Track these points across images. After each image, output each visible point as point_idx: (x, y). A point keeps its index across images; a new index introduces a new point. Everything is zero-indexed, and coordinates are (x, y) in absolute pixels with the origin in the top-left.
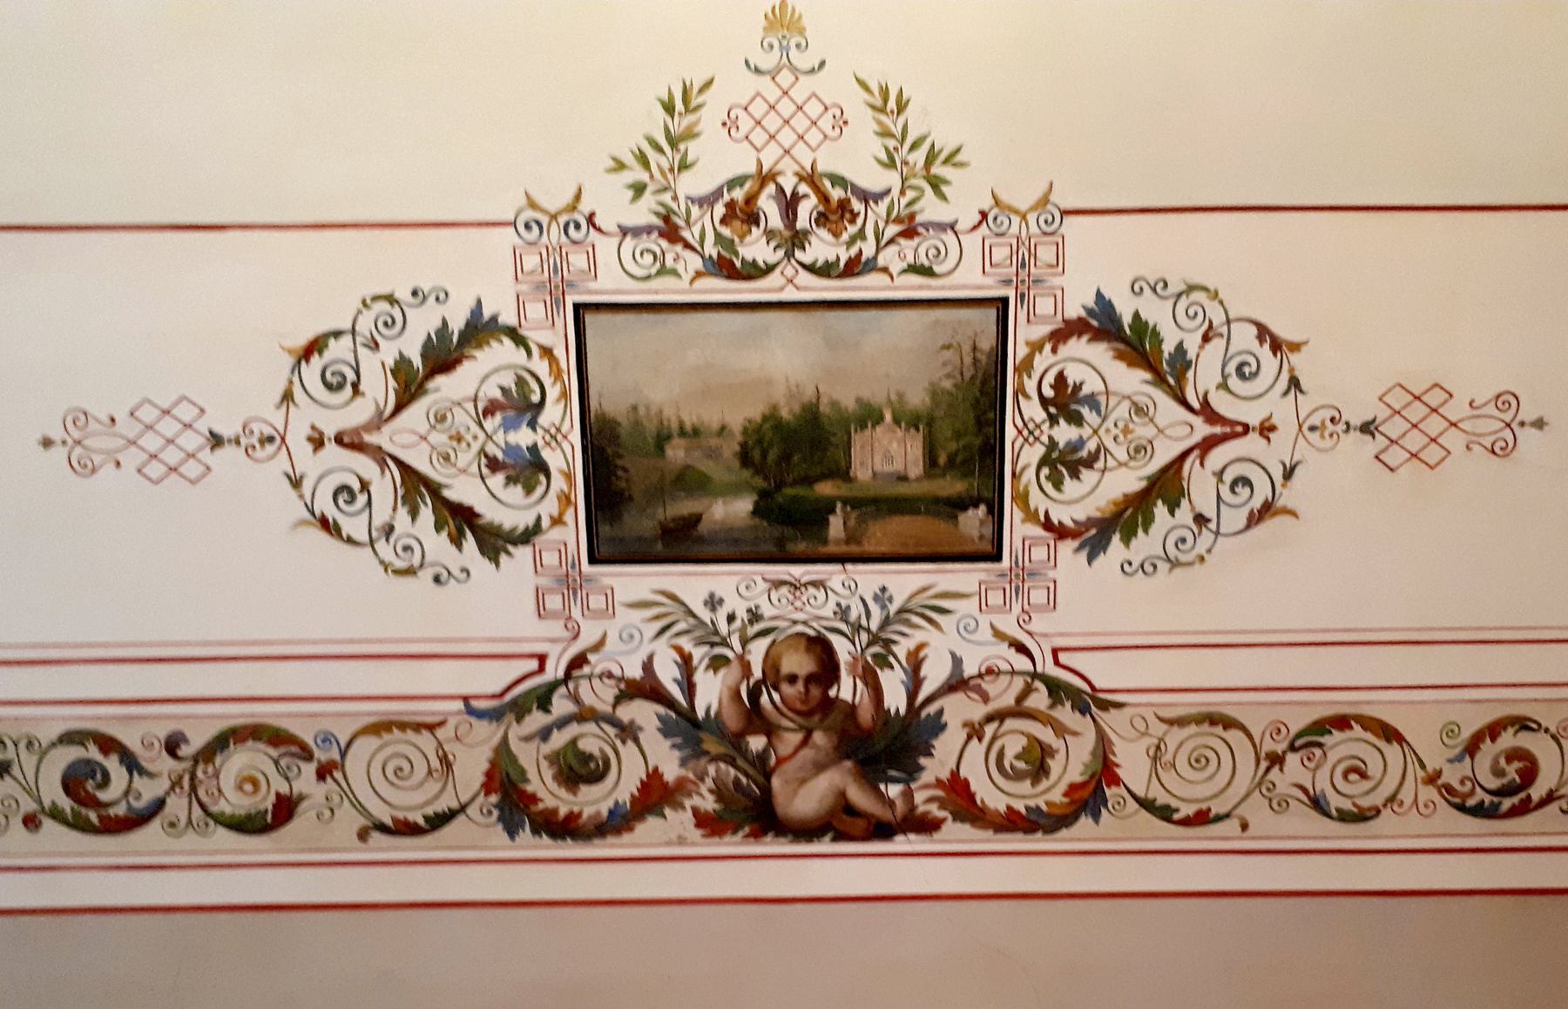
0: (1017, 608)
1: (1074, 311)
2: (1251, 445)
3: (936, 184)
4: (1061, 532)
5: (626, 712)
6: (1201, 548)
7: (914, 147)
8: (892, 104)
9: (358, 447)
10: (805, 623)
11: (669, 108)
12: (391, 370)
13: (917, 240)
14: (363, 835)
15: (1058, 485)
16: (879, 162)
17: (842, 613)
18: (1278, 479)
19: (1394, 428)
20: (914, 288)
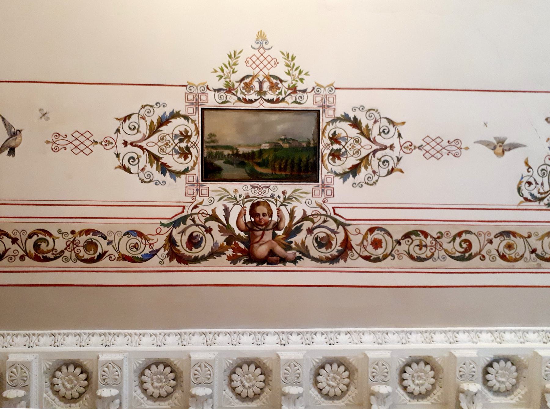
0: (323, 197)
1: (338, 115)
3: (302, 80)
5: (209, 224)
6: (374, 180)
7: (296, 69)
8: (290, 58)
9: (136, 146)
10: (261, 198)
11: (230, 57)
12: (149, 125)
13: (296, 94)
15: (335, 162)
16: (286, 73)
17: (272, 196)
19: (428, 148)
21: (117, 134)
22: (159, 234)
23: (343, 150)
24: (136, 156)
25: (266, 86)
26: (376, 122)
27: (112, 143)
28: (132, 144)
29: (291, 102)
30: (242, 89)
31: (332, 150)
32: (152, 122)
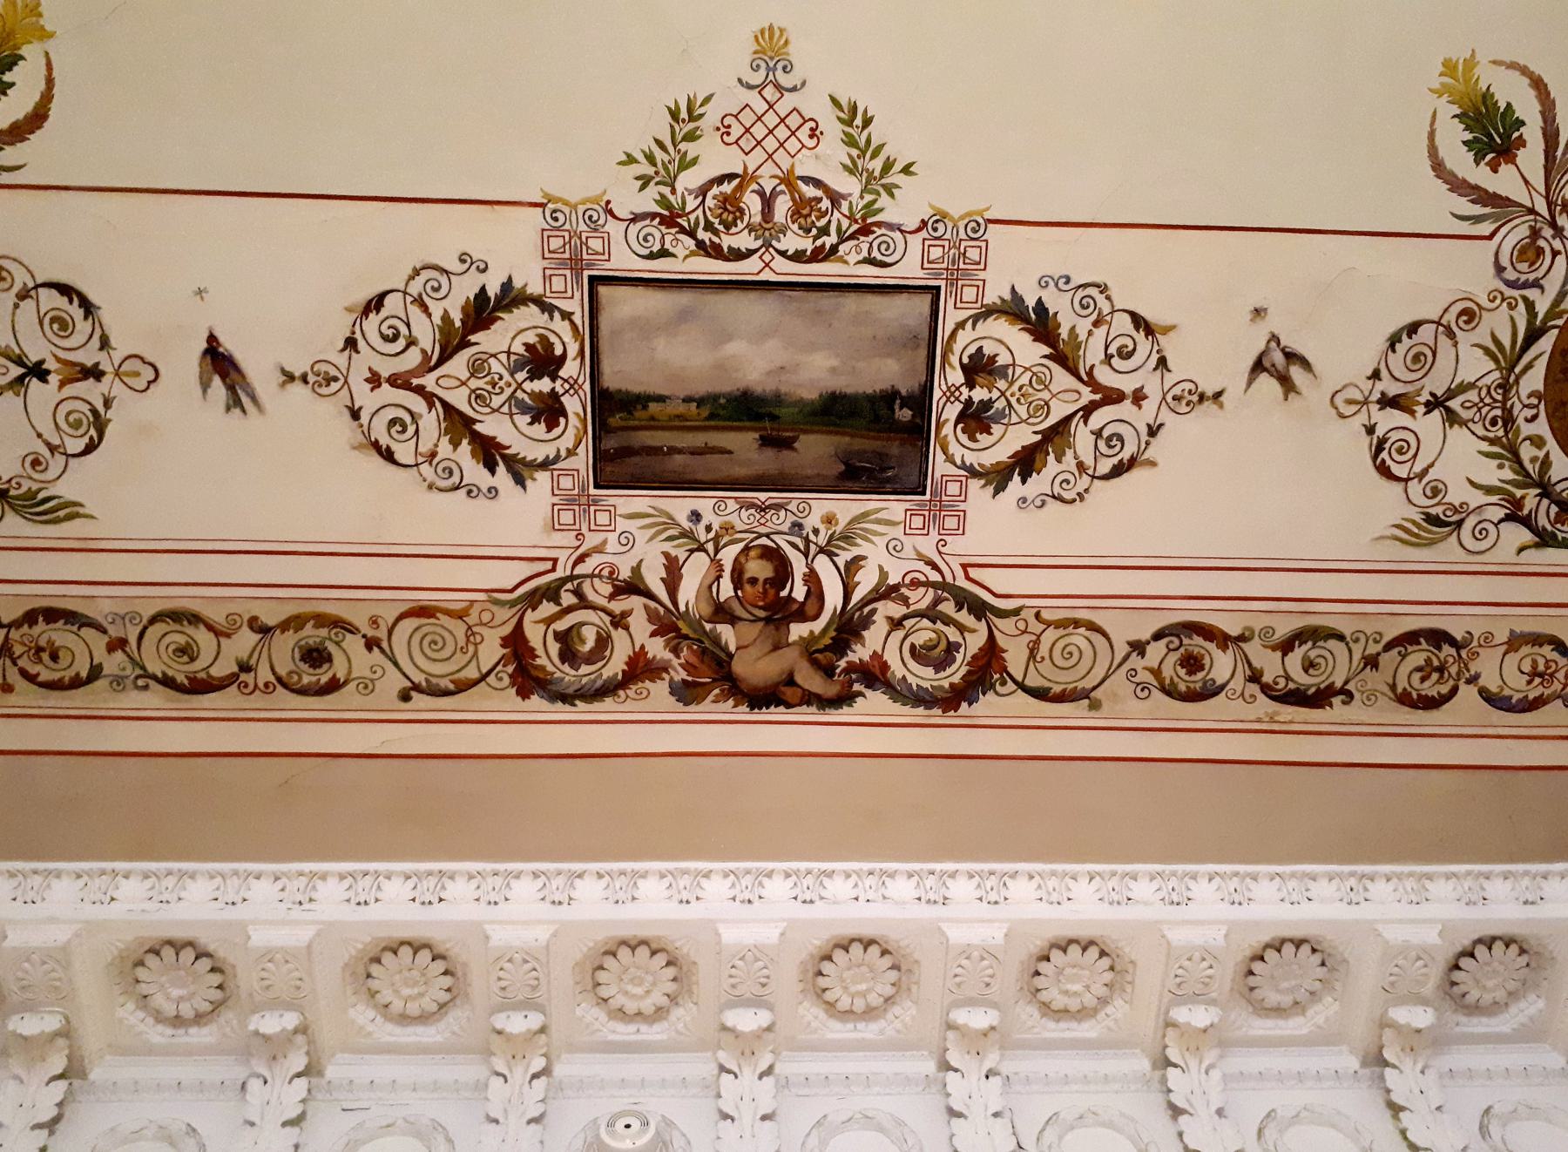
1: (991, 298)
2: (1125, 409)
3: (889, 189)
4: (973, 472)
6: (1080, 488)
7: (873, 157)
8: (858, 121)
9: (407, 386)
10: (767, 536)
11: (674, 115)
14: (405, 697)
18: (1144, 438)
20: (869, 274)
21: (347, 352)
22: (485, 625)
23: (1000, 404)
24: (408, 419)
25: (783, 206)
26: (1096, 324)
27: (336, 379)
28: (394, 381)
29: (856, 261)
30: (708, 213)
31: (969, 402)
32: (446, 317)
